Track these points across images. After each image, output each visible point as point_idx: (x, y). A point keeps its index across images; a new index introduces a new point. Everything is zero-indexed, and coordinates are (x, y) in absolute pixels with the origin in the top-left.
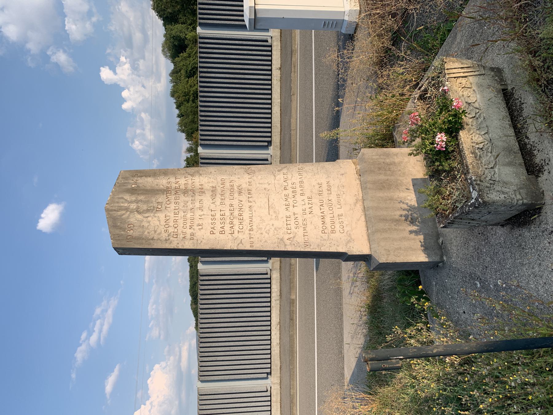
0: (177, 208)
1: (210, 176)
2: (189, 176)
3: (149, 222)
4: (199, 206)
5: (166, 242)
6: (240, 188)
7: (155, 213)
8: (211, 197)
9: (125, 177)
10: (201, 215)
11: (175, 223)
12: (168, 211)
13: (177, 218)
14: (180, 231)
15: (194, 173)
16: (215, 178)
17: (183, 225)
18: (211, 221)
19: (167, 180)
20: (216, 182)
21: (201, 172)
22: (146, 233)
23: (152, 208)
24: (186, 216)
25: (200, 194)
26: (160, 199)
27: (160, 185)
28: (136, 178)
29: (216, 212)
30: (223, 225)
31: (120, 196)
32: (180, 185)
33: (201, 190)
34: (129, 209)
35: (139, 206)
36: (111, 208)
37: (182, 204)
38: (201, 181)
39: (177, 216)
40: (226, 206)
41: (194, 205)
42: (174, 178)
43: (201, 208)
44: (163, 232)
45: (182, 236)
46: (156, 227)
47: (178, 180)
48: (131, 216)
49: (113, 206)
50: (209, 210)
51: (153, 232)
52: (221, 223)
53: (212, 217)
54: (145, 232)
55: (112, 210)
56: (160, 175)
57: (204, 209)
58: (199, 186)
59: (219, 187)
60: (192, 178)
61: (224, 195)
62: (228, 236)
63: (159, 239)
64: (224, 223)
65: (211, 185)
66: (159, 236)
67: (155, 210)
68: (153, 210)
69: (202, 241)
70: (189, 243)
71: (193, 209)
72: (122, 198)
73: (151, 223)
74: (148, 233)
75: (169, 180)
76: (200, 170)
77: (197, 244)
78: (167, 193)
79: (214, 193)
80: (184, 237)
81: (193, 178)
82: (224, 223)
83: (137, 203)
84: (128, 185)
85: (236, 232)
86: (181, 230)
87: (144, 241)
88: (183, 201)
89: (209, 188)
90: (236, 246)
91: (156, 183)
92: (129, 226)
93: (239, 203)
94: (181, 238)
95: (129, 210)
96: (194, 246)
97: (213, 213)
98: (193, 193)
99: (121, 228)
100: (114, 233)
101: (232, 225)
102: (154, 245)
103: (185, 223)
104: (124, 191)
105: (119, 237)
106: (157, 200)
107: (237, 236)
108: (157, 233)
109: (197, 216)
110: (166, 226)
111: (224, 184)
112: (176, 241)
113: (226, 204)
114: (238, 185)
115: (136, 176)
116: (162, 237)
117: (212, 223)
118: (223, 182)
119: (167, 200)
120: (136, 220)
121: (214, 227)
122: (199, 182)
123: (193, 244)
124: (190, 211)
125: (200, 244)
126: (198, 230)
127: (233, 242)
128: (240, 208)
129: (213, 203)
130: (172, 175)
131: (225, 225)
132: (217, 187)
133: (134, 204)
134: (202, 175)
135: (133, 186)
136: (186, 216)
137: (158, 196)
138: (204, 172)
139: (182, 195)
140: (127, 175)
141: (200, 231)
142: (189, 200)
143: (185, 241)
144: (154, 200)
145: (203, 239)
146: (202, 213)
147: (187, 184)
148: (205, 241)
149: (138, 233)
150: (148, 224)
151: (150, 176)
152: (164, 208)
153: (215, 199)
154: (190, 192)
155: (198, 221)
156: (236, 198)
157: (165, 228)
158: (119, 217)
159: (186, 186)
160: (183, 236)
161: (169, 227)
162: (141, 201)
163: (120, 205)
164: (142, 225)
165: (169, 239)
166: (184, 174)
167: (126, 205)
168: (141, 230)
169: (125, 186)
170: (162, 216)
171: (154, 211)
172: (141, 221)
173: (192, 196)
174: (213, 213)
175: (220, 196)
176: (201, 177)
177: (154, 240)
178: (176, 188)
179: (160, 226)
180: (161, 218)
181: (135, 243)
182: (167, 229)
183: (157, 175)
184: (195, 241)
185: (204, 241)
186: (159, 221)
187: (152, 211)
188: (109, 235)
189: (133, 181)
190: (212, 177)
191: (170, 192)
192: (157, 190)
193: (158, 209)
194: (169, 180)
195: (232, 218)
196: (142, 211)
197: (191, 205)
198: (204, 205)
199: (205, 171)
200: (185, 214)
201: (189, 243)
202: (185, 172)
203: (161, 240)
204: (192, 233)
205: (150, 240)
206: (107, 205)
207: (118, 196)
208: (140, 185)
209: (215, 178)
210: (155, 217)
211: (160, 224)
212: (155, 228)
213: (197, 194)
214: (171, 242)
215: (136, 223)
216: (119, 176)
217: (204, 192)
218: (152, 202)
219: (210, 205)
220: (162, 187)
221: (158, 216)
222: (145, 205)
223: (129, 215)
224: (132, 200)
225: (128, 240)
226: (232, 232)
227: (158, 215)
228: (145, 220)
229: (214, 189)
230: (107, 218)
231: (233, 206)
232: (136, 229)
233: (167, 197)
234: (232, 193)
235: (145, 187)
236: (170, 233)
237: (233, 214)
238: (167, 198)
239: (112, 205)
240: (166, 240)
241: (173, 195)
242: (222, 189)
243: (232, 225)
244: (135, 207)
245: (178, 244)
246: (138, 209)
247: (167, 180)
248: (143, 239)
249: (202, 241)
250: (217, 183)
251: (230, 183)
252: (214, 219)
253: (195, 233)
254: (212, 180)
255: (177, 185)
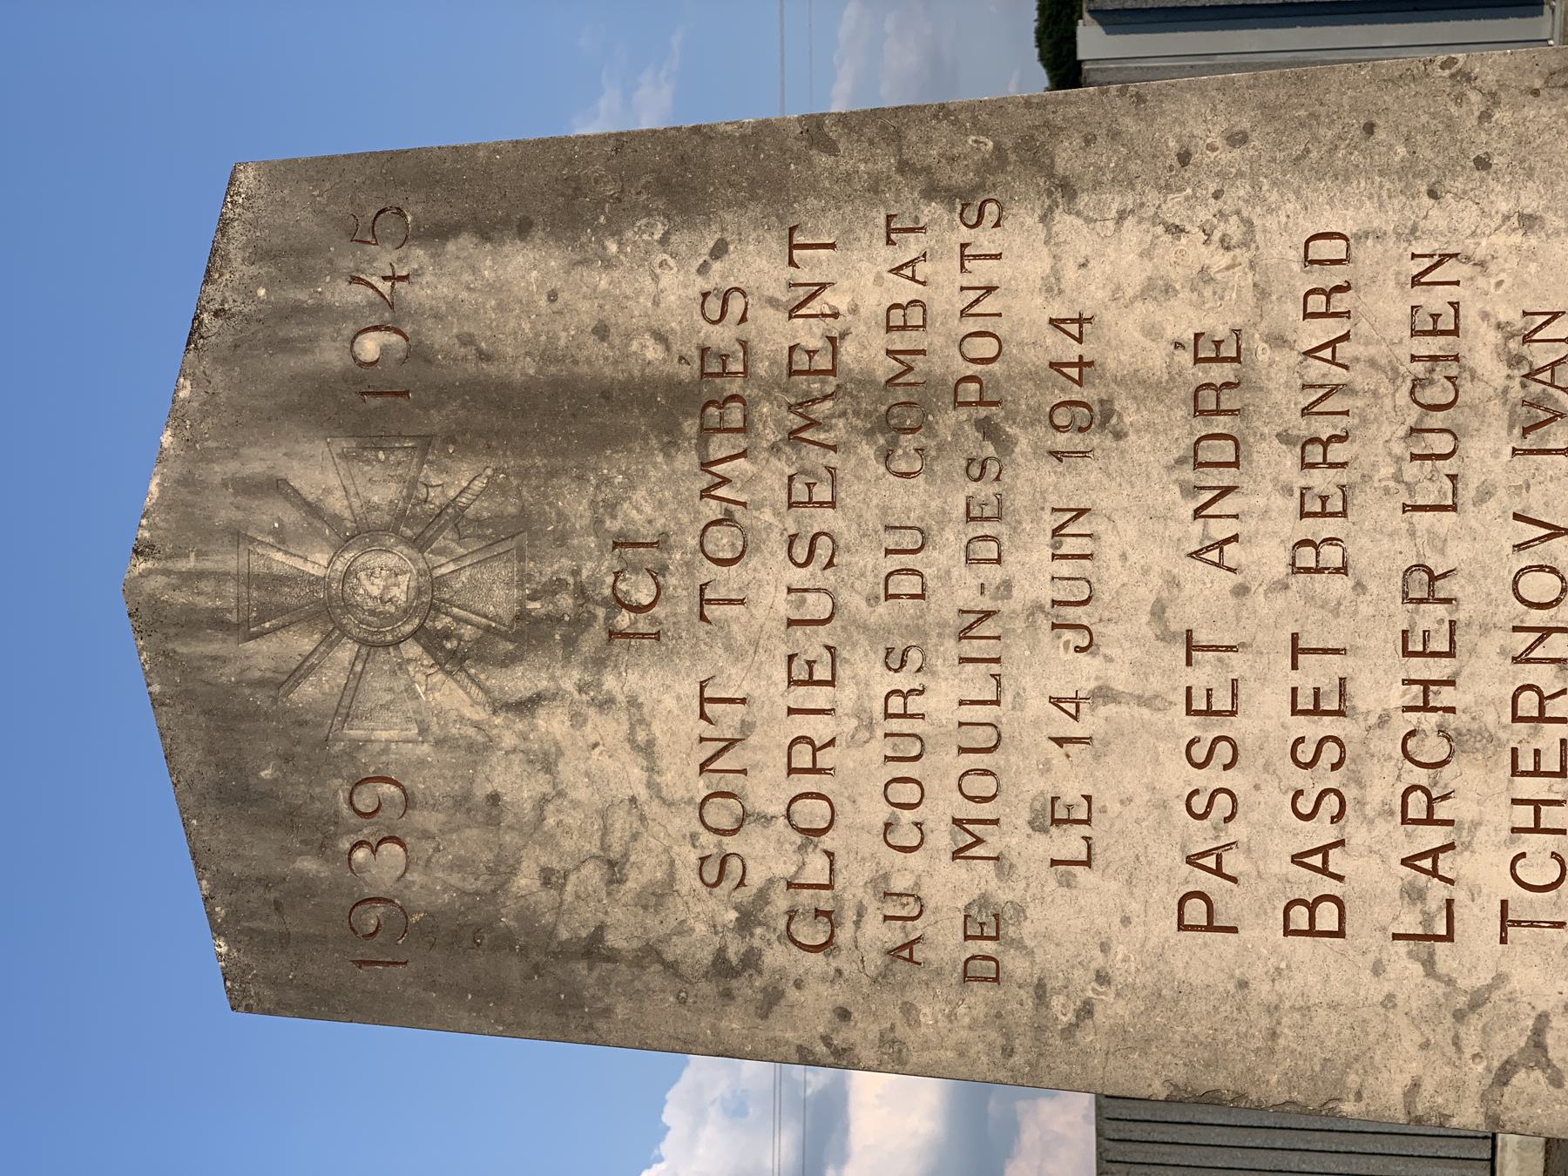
0: (818, 606)
1: (1173, 207)
2: (932, 211)
3: (547, 762)
4: (1047, 594)
5: (728, 995)
6: (1541, 355)
7: (599, 663)
8: (1188, 474)
9: (277, 240)
10: (1076, 701)
11: (809, 783)
12: (728, 648)
13: (819, 728)
14: (854, 884)
15: (985, 167)
16: (1233, 228)
17: (884, 812)
18: (1179, 777)
19: (703, 269)
20: (1243, 279)
21: (1066, 156)
22: (526, 880)
23: (566, 602)
24: (915, 705)
25: (1061, 441)
26: (639, 495)
27: (628, 336)
28: (384, 259)
29: (1238, 664)
30: (1322, 831)
31: (257, 462)
32: (836, 327)
33: (1076, 393)
34: (349, 607)
35: (438, 583)
36: (181, 598)
37: (868, 562)
38: (1071, 274)
39: (819, 697)
40: (1360, 587)
41: (993, 574)
42: (777, 245)
43: (1071, 614)
44: (688, 879)
45: (877, 934)
46: (621, 822)
47: (815, 266)
48: (378, 687)
49: (201, 575)
50: (1166, 637)
51: (593, 875)
52: (1305, 806)
53: (1190, 727)
54: (514, 870)
55: (194, 623)
56: (621, 215)
57: (1111, 630)
58: (1053, 338)
59: (1278, 341)
60: (965, 234)
61: (1337, 452)
62: (1378, 969)
63: (650, 953)
64: (1331, 803)
65: (1182, 320)
66: (656, 926)
67: (598, 628)
68: (581, 623)
69: (1086, 1010)
70: (952, 1017)
71: (987, 628)
72: (277, 487)
73: (565, 770)
74: (548, 877)
75: (719, 274)
76: (1055, 131)
77: (1040, 1029)
78: (706, 432)
79: (1221, 424)
80: (903, 952)
81: (984, 239)
82: (1331, 803)
83: (419, 544)
84: (313, 339)
85: (1478, 922)
86: (867, 871)
87: (513, 969)
88: (872, 519)
89: (1157, 359)
90: (1474, 1088)
91: (587, 313)
92: (365, 801)
93: (1526, 559)
94: (875, 961)
95: (349, 621)
96: (1008, 1052)
97: (1205, 674)
98: (988, 429)
99: (290, 819)
100: (236, 868)
101: (1433, 837)
102: (607, 1012)
103: (908, 793)
104: (289, 410)
105: (277, 905)
106: (612, 507)
107: (1483, 978)
108: (634, 882)
109: (1038, 705)
110: (720, 814)
111: (1340, 302)
112: (824, 990)
113: (1359, 562)
114: (1509, 313)
115: (388, 224)
116: (682, 929)
117: (1199, 804)
118: (1335, 277)
119: (713, 510)
120: (423, 730)
121: (1218, 852)
122: (1052, 288)
123: (993, 1035)
124: (951, 648)
125: (1069, 1031)
126: (1050, 877)
127: (1441, 1036)
128: (1537, 618)
129: (1210, 552)
130: (755, 210)
131: (1354, 829)
132: (1263, 354)
133: (390, 560)
134: (1084, 200)
135: (370, 347)
136: (915, 705)
137: (615, 466)
138: (1106, 156)
139: (867, 450)
140: (303, 219)
141: (1067, 883)
142: (943, 515)
143: (915, 995)
144: (575, 504)
145: (1102, 978)
146: (1084, 673)
147: (915, 317)
148: (1121, 1009)
149: (454, 879)
150: (540, 785)
151: (524, 230)
152: (685, 606)
153: (1228, 505)
154: (949, 420)
155: (1047, 768)
156: (1485, 494)
157: (707, 839)
158: (261, 699)
159: (900, 342)
160: (894, 936)
161: (741, 822)
162: (453, 517)
163: (258, 566)
164: (481, 791)
165: (751, 960)
166: (875, 187)
167: (317, 562)
168: (472, 840)
169: (286, 345)
170: (669, 702)
171: (590, 641)
172: (471, 747)
173: (977, 469)
174: (1205, 674)
175: (1291, 459)
176: (1064, 222)
177: (613, 957)
178: (802, 361)
179: (654, 809)
180: (657, 728)
181: (432, 986)
182: (731, 845)
183: (599, 204)
184: (1020, 1007)
185: (1113, 1009)
186: (647, 750)
187: (570, 643)
188: (189, 889)
189: (359, 295)
190: (1203, 215)
191: (735, 415)
192: (606, 395)
193: (624, 620)
194: (719, 274)
195: (1434, 749)
196: (468, 632)
197: (960, 570)
198: (1112, 575)
199: (1114, 135)
200: (903, 681)
201: (952, 1017)
202: (885, 163)
203: (672, 968)
204: (983, 901)
205: (564, 953)
206: (143, 566)
207: (232, 467)
208: (440, 337)
209: (1233, 228)
210: (605, 704)
211: (650, 785)
212: (605, 831)
213: (1023, 445)
214: (771, 999)
215: (422, 763)
216: (224, 225)
217: (1101, 418)
218: (562, 539)
219: (1173, 582)
220: (653, 352)
221: (633, 702)
222: (503, 570)
223: (356, 679)
224: (370, 507)
225: (365, 951)
226: (1428, 919)
227: (633, 677)
228: (509, 740)
229: (1219, 373)
230: (156, 702)
231: (1444, 588)
232: (426, 835)
233: (705, 481)
234: (1437, 420)
235: (484, 356)
236: (763, 896)
237: (1445, 697)
238: (706, 493)
239: (190, 563)
240: (722, 968)
241: (775, 449)
242: (1316, 370)
243: (1433, 837)
244: (399, 593)
245: (844, 1014)
246: (435, 608)
247: (703, 269)
248: (505, 942)
249: (1086, 1010)
250: (1262, 293)
251: (1419, 296)
252: (1224, 751)
253: (1020, 910)
254: (1195, 252)
255: (810, 334)
